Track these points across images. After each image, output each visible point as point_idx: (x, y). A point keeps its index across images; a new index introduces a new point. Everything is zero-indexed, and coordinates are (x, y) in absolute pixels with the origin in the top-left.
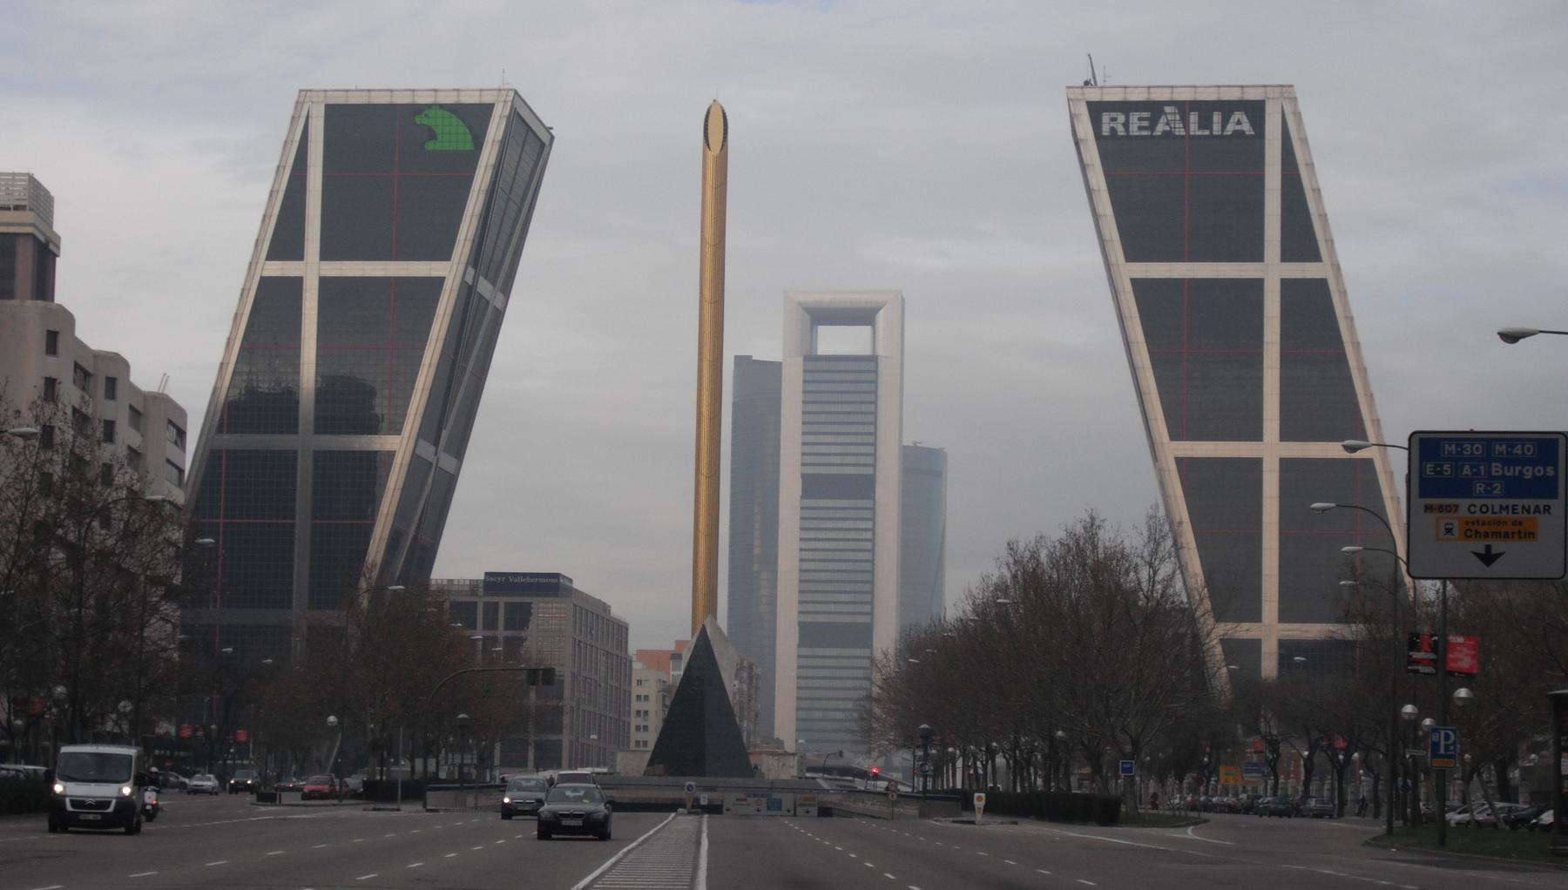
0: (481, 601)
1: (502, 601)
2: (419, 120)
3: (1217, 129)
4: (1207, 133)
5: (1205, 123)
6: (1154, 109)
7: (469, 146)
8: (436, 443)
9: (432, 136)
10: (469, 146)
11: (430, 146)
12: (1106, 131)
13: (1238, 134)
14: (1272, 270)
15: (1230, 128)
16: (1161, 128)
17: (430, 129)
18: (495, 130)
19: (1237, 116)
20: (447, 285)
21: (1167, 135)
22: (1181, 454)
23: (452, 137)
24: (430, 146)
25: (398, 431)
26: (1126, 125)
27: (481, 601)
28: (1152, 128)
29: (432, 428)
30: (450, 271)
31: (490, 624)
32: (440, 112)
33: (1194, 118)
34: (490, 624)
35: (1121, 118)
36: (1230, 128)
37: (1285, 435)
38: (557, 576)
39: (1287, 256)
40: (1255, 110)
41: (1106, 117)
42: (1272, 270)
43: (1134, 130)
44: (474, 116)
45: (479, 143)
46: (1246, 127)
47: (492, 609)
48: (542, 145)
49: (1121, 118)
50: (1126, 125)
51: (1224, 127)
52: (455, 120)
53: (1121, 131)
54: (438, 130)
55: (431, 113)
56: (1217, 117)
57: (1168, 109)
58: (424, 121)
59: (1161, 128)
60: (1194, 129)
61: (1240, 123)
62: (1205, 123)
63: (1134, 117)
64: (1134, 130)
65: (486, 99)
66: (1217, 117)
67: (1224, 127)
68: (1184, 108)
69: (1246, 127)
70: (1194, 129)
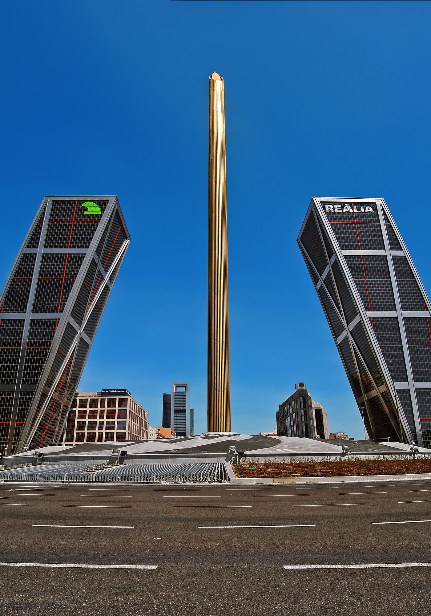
0: (99, 398)
1: (106, 398)
2: (82, 205)
3: (363, 211)
5: (359, 209)
6: (343, 204)
7: (100, 213)
8: (80, 325)
9: (87, 209)
10: (100, 213)
11: (85, 213)
12: (327, 210)
13: (369, 212)
15: (367, 211)
16: (345, 210)
19: (368, 207)
21: (347, 212)
23: (93, 209)
24: (85, 213)
25: (62, 310)
26: (334, 209)
27: (99, 398)
28: (342, 210)
29: (77, 313)
30: (90, 252)
31: (102, 405)
32: (90, 203)
33: (355, 207)
34: (102, 405)
35: (332, 207)
36: (367, 211)
38: (125, 390)
40: (374, 205)
41: (327, 206)
43: (336, 210)
45: (103, 211)
46: (372, 210)
47: (103, 401)
49: (332, 207)
50: (334, 209)
51: (365, 210)
53: (332, 210)
54: (89, 208)
55: (87, 203)
56: (362, 207)
57: (346, 205)
58: (85, 205)
59: (345, 210)
61: (369, 209)
63: (336, 207)
64: (336, 210)
66: (362, 207)
67: (365, 210)
68: (351, 204)
70: (355, 210)
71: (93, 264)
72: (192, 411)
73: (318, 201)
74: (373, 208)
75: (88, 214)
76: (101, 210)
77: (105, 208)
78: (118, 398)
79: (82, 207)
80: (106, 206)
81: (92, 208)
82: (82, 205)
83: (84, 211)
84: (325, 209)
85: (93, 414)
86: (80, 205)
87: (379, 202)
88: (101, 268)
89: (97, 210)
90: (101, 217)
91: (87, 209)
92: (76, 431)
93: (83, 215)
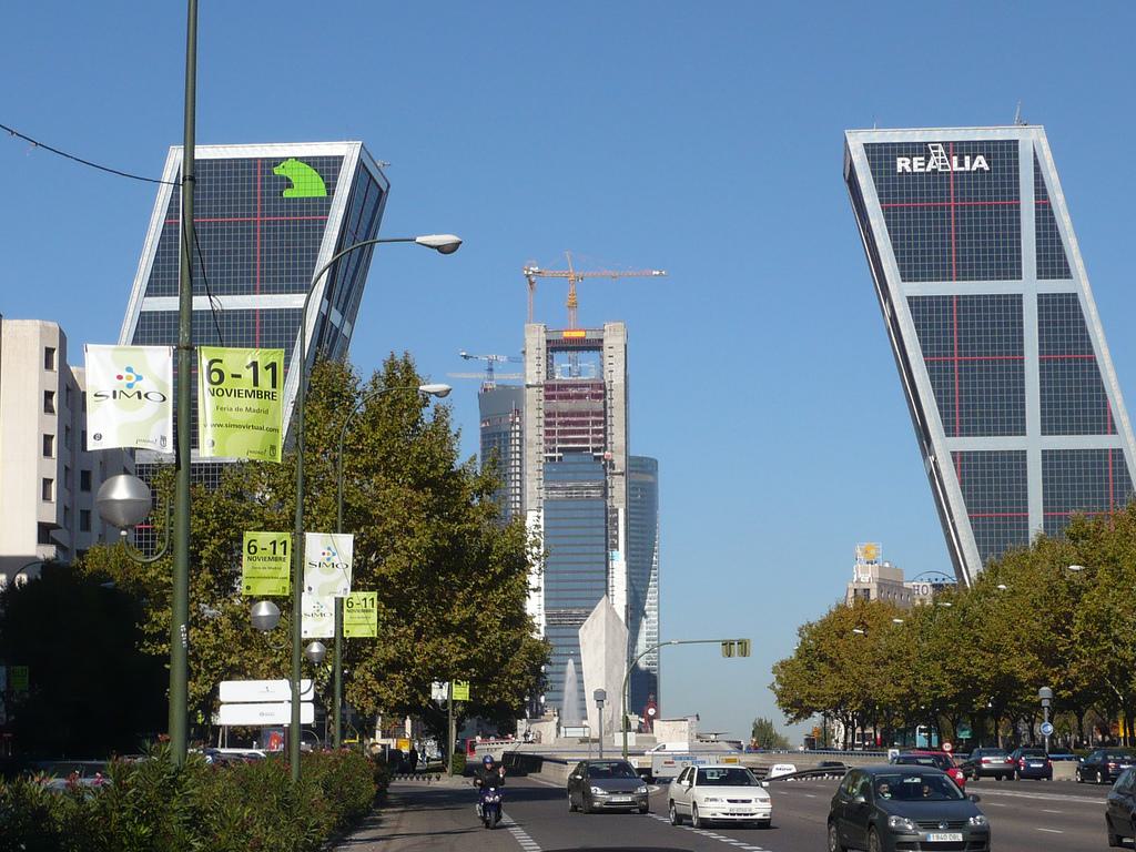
2: (277, 171)
7: (323, 193)
9: (290, 186)
10: (323, 193)
11: (287, 194)
14: (1029, 287)
17: (288, 180)
21: (935, 171)
23: (307, 185)
24: (287, 194)
42: (1029, 287)
44: (328, 168)
45: (331, 187)
48: (381, 191)
52: (310, 171)
60: (956, 168)
71: (323, 320)
72: (642, 472)
73: (857, 141)
75: (295, 199)
76: (328, 185)
77: (336, 178)
79: (276, 178)
80: (336, 171)
81: (302, 179)
82: (277, 171)
83: (282, 187)
86: (270, 172)
87: (1032, 140)
88: (335, 317)
89: (315, 186)
90: (329, 207)
91: (290, 186)
93: (282, 200)
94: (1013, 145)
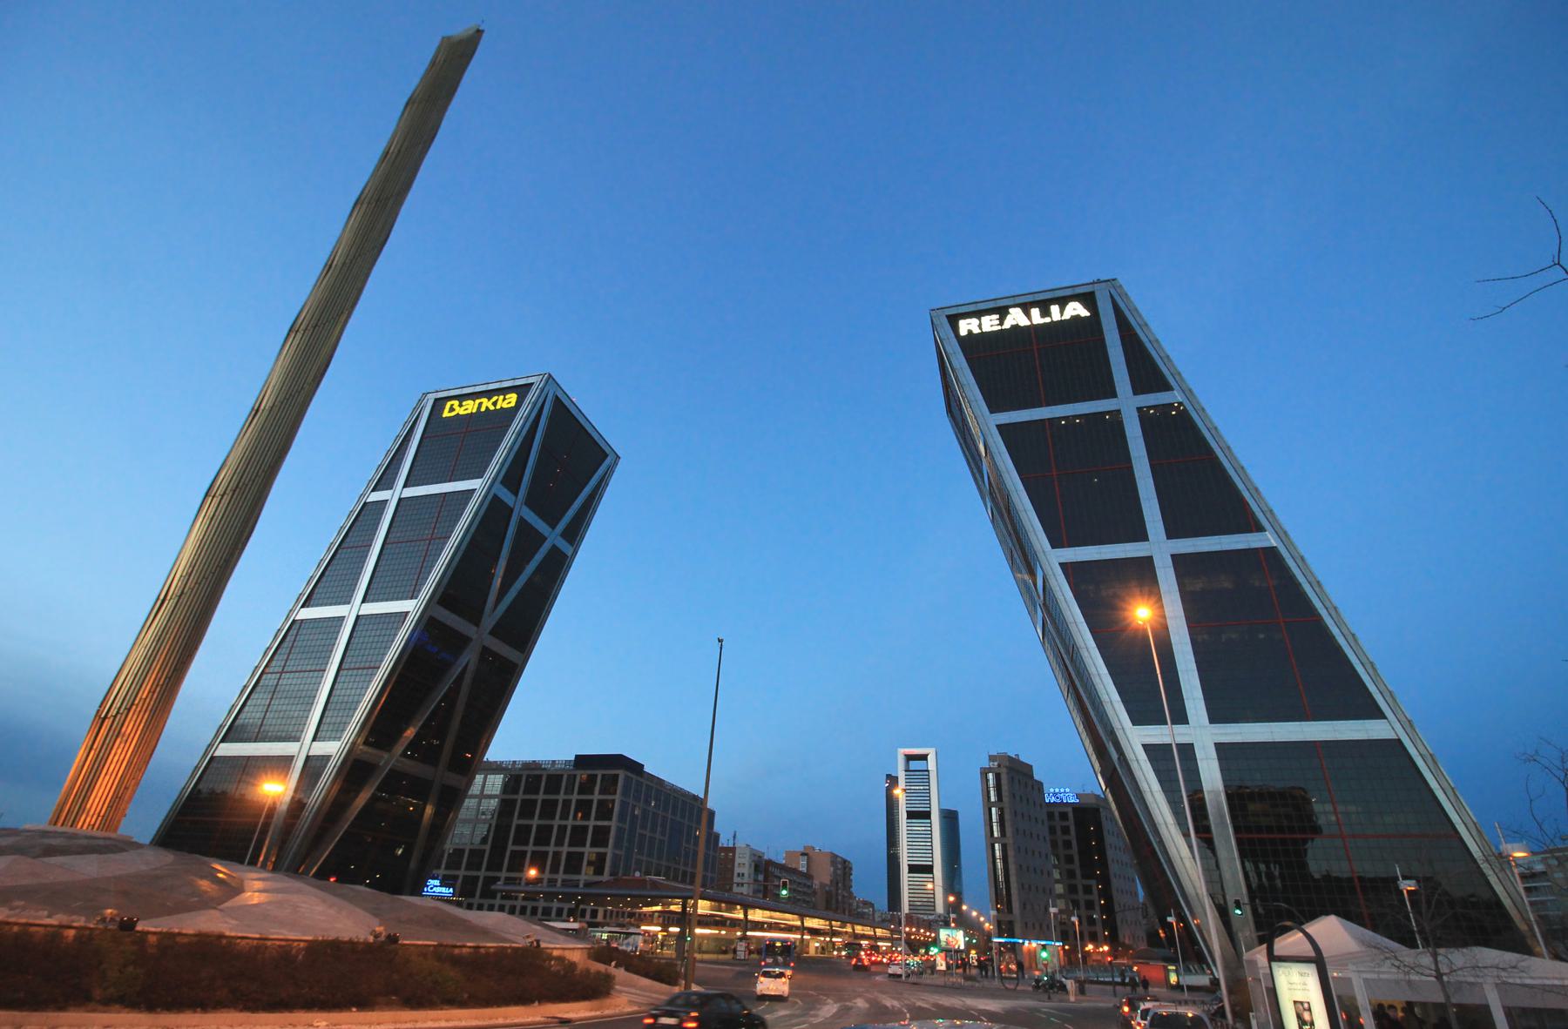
4: (1048, 320)
5: (1045, 312)
12: (963, 332)
13: (1076, 318)
18: (531, 397)
20: (476, 495)
22: (1063, 560)
26: (980, 326)
28: (1001, 324)
33: (1035, 312)
37: (1172, 533)
39: (1138, 388)
42: (1127, 403)
46: (1084, 313)
49: (975, 321)
50: (980, 326)
61: (1076, 309)
62: (1045, 312)
65: (530, 380)
66: (1055, 309)
69: (1084, 313)
74: (1086, 307)
78: (599, 773)
84: (955, 329)
85: (549, 809)
92: (510, 847)
94: (1092, 294)
